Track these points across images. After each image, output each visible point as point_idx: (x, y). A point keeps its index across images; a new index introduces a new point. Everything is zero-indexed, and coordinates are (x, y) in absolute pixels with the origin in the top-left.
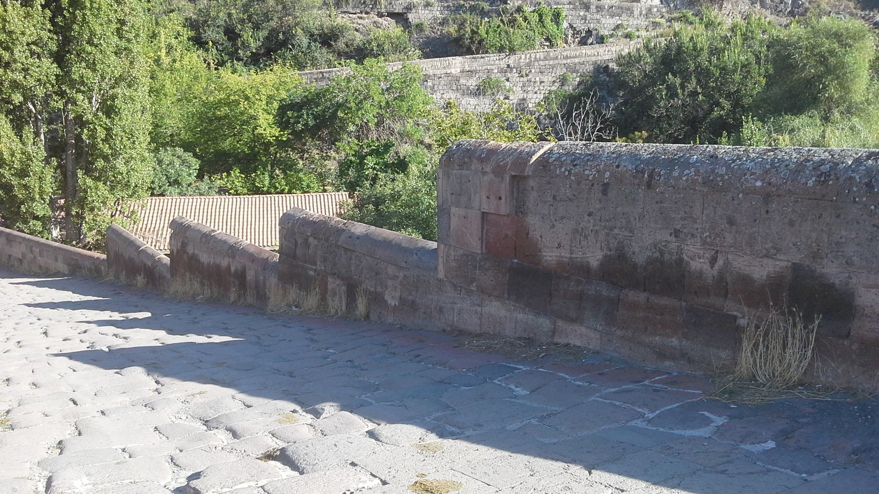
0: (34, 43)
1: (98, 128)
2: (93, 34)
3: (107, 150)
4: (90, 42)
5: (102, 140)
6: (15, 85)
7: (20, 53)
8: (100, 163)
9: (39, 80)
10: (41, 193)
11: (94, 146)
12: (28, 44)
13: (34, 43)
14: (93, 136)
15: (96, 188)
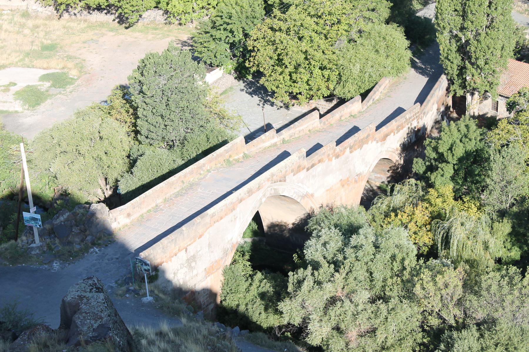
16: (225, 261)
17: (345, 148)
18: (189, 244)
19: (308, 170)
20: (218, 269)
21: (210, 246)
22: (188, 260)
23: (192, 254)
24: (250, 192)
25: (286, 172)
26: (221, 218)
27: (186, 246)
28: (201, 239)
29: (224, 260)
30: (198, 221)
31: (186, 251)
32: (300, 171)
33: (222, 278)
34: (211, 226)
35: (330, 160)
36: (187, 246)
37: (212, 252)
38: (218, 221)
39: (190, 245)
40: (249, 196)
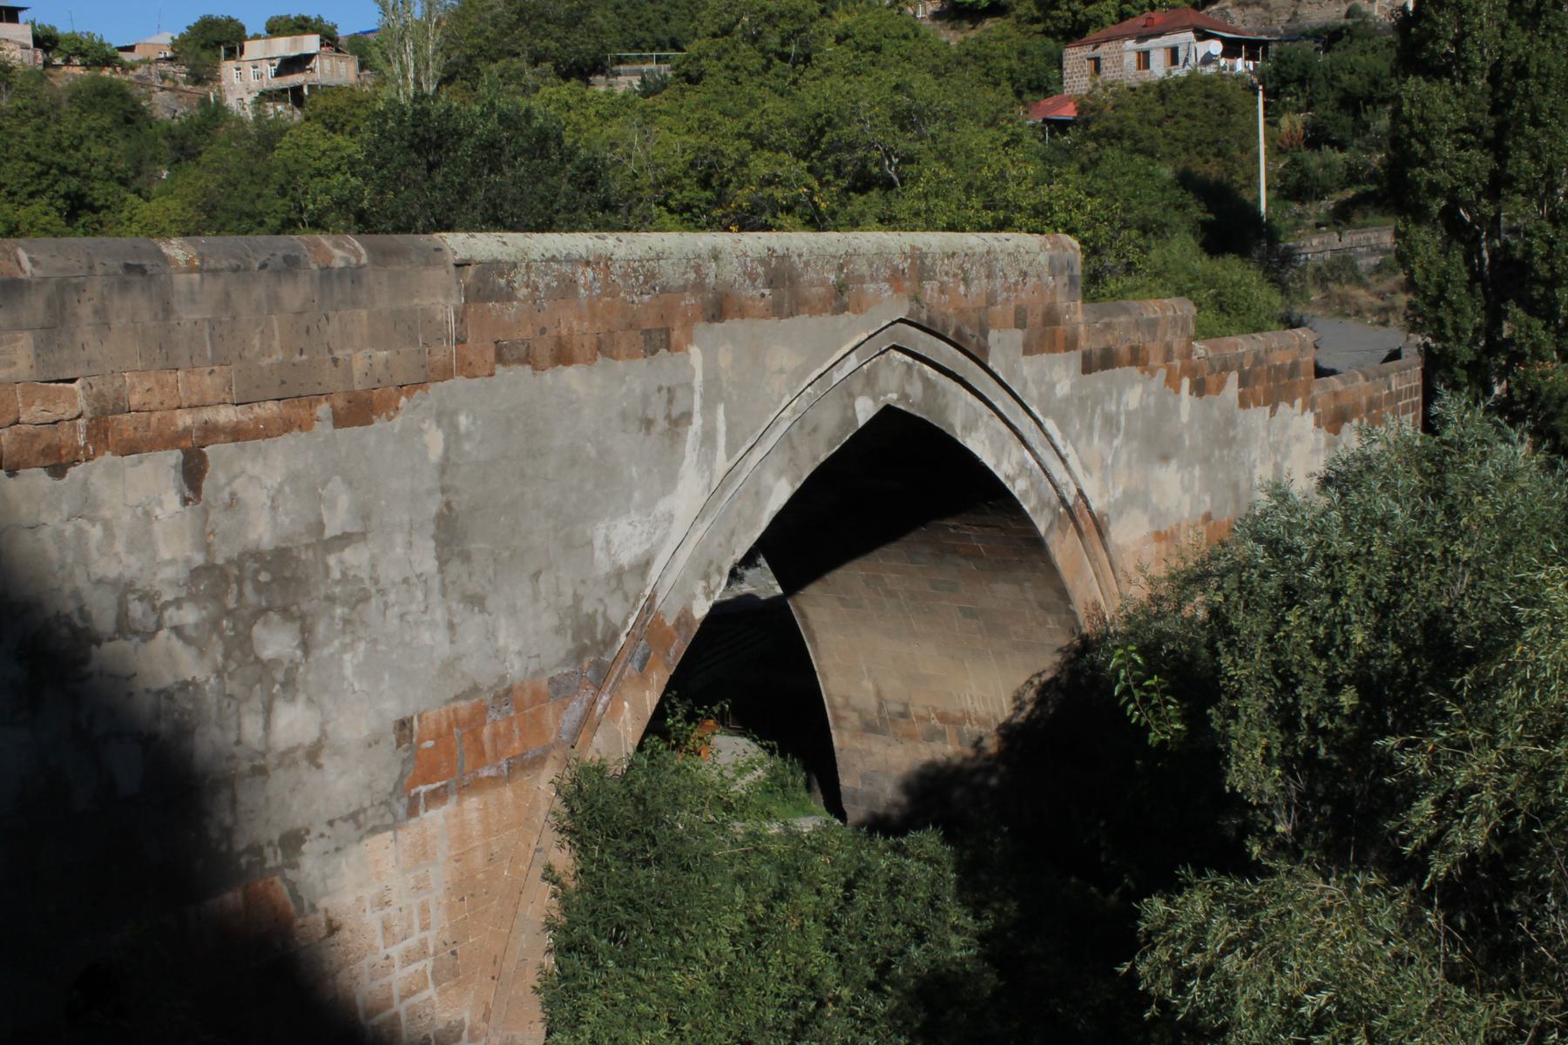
0: (1464, 130)
1: (1535, 242)
2: (1535, 110)
3: (1543, 270)
4: (1535, 123)
5: (1544, 259)
6: (1434, 190)
7: (1446, 148)
8: (1538, 292)
9: (1466, 178)
10: (1456, 329)
11: (1530, 267)
12: (1457, 131)
13: (1464, 130)
14: (1528, 253)
15: (1529, 327)
16: (588, 722)
17: (1226, 368)
18: (226, 415)
19: (1088, 367)
20: (527, 764)
21: (449, 533)
22: (210, 579)
23: (262, 532)
24: (784, 290)
25: (991, 299)
26: (563, 356)
27: (185, 419)
28: (368, 435)
29: (576, 708)
30: (339, 258)
31: (193, 473)
32: (1053, 349)
33: (564, 860)
34: (468, 369)
35: (1172, 382)
36: (210, 432)
37: (476, 601)
38: (527, 359)
39: (237, 434)
40: (778, 310)
